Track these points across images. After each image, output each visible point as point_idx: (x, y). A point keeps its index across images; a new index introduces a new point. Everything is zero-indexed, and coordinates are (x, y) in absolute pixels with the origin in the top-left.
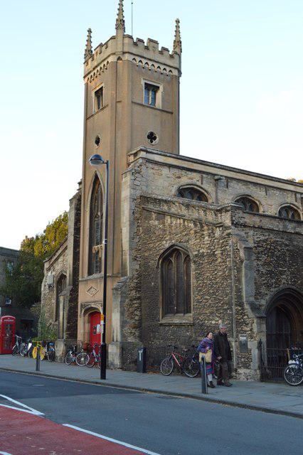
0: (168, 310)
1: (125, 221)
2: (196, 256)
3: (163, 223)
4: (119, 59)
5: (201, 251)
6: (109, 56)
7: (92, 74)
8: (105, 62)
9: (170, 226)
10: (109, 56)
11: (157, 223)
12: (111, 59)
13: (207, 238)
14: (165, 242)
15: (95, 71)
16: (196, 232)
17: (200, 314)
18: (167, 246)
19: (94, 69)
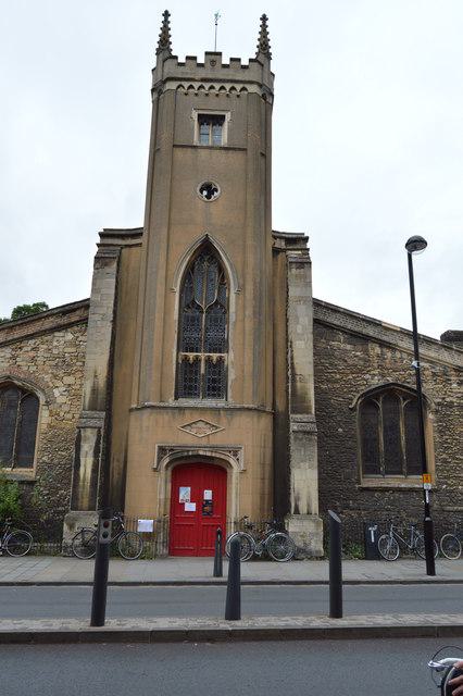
0: (371, 468)
2: (439, 404)
3: (366, 352)
4: (264, 96)
5: (448, 400)
6: (251, 82)
7: (196, 85)
8: (239, 87)
9: (381, 357)
10: (251, 82)
11: (349, 347)
12: (253, 89)
13: (455, 385)
14: (367, 376)
15: (207, 86)
16: (434, 374)
17: (448, 478)
18: (376, 382)
19: (204, 80)
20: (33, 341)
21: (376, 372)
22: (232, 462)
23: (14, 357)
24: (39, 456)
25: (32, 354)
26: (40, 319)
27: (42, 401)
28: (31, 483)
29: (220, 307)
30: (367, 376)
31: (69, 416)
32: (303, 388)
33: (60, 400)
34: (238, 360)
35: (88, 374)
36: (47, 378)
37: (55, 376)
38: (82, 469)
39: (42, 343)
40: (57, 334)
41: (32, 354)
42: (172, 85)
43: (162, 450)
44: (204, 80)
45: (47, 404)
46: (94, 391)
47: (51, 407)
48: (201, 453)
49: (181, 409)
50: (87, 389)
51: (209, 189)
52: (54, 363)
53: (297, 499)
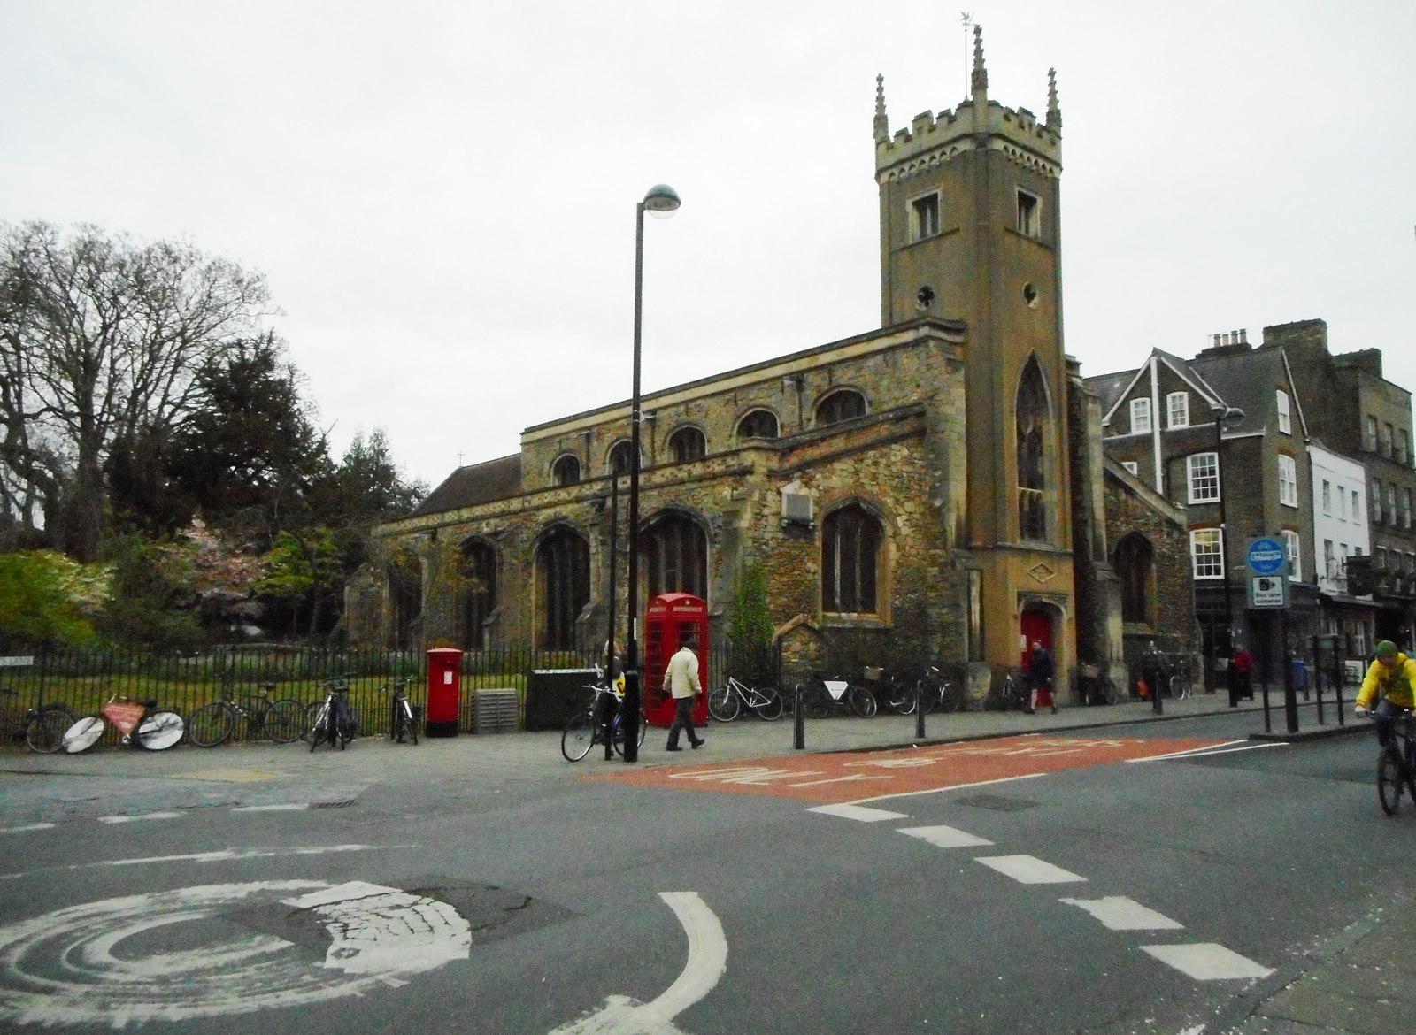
1: (1095, 472)
15: (1026, 155)
19: (1024, 148)
20: (871, 453)
21: (1122, 519)
22: (1063, 609)
23: (857, 472)
24: (888, 597)
25: (873, 469)
26: (875, 424)
27: (889, 531)
28: (887, 631)
29: (1037, 435)
30: (1118, 523)
31: (913, 552)
32: (1100, 533)
33: (905, 531)
34: (1054, 498)
35: (952, 505)
36: (890, 501)
37: (897, 501)
38: (973, 615)
39: (881, 457)
40: (893, 446)
41: (873, 469)
42: (999, 145)
43: (1020, 596)
44: (1024, 148)
45: (895, 535)
46: (958, 526)
47: (898, 539)
48: (1044, 600)
49: (1030, 551)
50: (952, 522)
51: (1029, 295)
52: (894, 483)
53: (1112, 646)
